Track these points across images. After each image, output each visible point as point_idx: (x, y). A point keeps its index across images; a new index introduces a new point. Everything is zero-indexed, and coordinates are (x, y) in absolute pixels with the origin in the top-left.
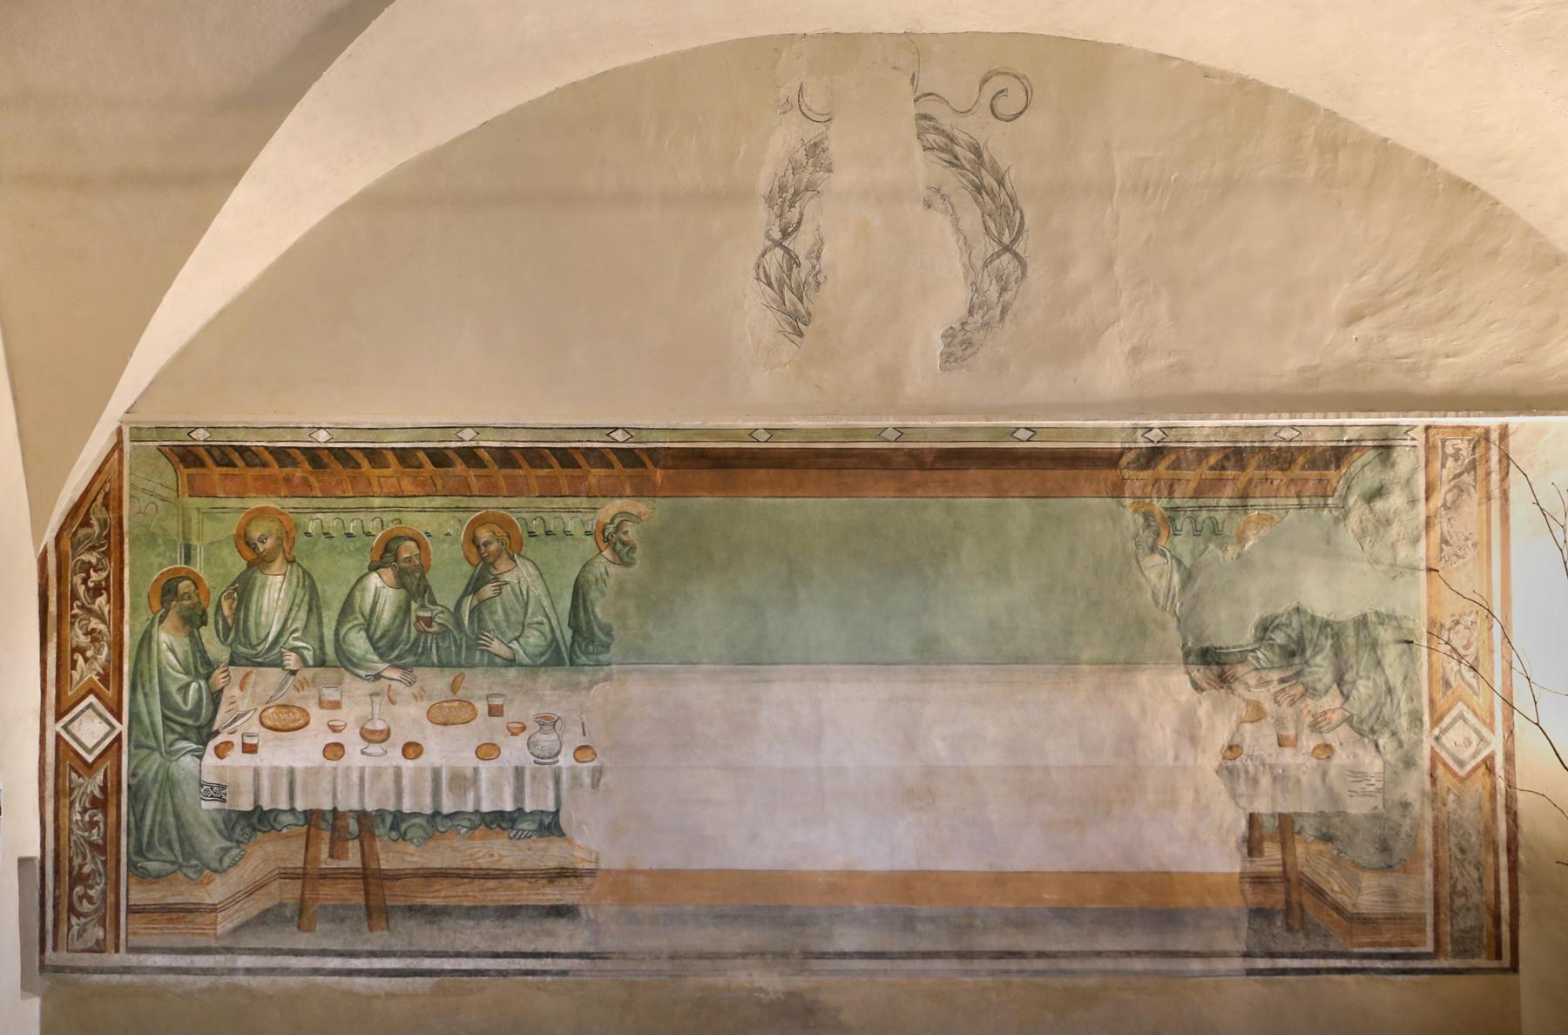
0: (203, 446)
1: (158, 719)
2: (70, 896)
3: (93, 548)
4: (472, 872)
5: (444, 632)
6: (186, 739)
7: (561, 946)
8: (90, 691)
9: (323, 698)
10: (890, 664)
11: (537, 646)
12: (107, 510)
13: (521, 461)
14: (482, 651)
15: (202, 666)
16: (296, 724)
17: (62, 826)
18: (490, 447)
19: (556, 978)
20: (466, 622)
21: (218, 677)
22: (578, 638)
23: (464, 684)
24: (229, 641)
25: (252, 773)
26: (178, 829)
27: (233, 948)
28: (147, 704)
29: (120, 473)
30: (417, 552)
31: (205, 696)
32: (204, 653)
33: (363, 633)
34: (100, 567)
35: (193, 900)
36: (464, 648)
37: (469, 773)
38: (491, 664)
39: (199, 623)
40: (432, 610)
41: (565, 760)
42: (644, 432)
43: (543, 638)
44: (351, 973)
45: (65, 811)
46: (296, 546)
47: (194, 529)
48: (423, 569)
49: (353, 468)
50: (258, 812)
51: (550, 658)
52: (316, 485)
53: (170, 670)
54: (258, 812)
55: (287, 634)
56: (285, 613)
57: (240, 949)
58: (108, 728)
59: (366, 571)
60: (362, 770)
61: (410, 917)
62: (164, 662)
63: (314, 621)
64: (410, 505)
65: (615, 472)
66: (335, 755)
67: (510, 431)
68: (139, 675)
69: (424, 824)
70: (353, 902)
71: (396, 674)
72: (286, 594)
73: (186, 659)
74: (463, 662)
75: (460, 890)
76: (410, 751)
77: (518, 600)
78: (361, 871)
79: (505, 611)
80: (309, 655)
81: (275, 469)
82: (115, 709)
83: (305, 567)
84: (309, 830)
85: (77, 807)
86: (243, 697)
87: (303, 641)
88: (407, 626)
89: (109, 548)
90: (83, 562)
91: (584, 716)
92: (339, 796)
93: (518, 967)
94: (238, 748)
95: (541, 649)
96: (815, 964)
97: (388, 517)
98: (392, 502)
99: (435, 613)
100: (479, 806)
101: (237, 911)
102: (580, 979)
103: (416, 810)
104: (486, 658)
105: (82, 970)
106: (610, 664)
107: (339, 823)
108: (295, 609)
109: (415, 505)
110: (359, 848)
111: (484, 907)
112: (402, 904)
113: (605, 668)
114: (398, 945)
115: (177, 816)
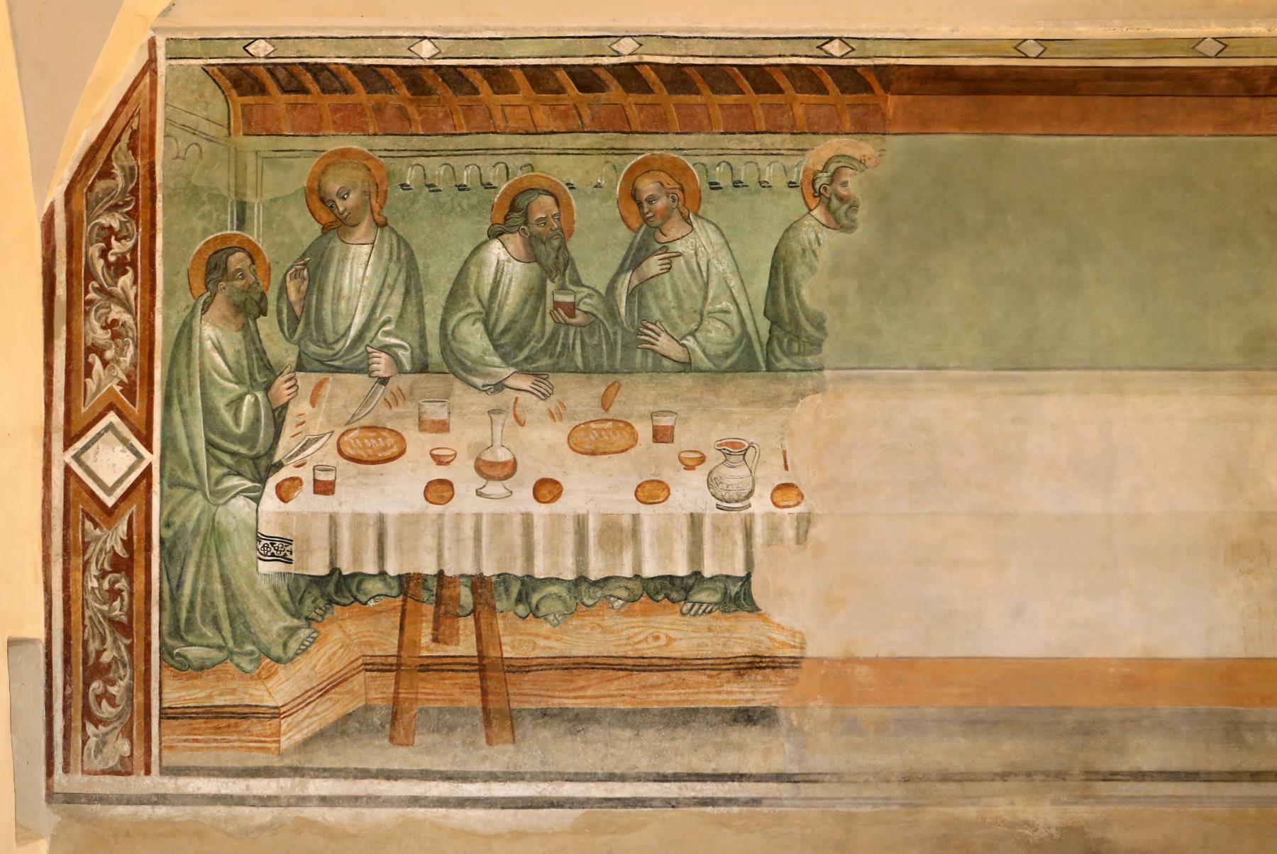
0: (264, 64)
1: (201, 445)
2: (85, 696)
3: (115, 207)
4: (630, 662)
5: (592, 323)
6: (239, 474)
7: (752, 765)
8: (111, 407)
9: (425, 417)
10: (1207, 370)
12: (135, 154)
13: (700, 84)
14: (645, 351)
15: (259, 372)
16: (388, 454)
17: (73, 597)
19: (745, 809)
20: (623, 310)
21: (282, 388)
22: (777, 332)
24: (296, 337)
26: (227, 602)
27: (303, 769)
28: (186, 425)
29: (153, 103)
30: (555, 210)
31: (263, 413)
32: (262, 353)
33: (479, 326)
34: (124, 233)
35: (247, 702)
36: (619, 346)
37: (626, 522)
38: (658, 369)
39: (255, 311)
40: (575, 293)
41: (761, 505)
42: (869, 44)
43: (729, 333)
44: (462, 803)
45: (77, 575)
46: (388, 203)
47: (251, 179)
48: (564, 235)
50: (335, 578)
51: (739, 358)
52: (417, 117)
53: (217, 377)
54: (335, 578)
55: (375, 328)
56: (372, 298)
57: (312, 769)
58: (134, 458)
59: (485, 237)
60: (478, 517)
61: (544, 725)
62: (208, 365)
63: (412, 308)
64: (546, 145)
67: (685, 42)
68: (175, 384)
69: (564, 594)
70: (465, 705)
71: (525, 383)
72: (375, 271)
73: (238, 362)
74: (618, 366)
75: (613, 687)
76: (544, 491)
77: (694, 278)
78: (476, 661)
80: (404, 356)
81: (361, 95)
82: (144, 432)
83: (400, 233)
84: (405, 601)
85: (94, 570)
86: (315, 416)
87: (397, 337)
88: (540, 314)
89: (136, 207)
90: (103, 228)
91: (786, 443)
93: (693, 794)
94: (308, 486)
95: (725, 348)
96: (1102, 788)
97: (515, 162)
98: (519, 141)
99: (579, 296)
100: (640, 570)
101: (307, 717)
102: (777, 810)
104: (650, 360)
105: (102, 800)
107: (446, 592)
108: (387, 292)
109: (552, 146)
110: (474, 629)
111: (644, 711)
112: (534, 707)
113: (815, 374)
114: (528, 763)
115: (226, 582)
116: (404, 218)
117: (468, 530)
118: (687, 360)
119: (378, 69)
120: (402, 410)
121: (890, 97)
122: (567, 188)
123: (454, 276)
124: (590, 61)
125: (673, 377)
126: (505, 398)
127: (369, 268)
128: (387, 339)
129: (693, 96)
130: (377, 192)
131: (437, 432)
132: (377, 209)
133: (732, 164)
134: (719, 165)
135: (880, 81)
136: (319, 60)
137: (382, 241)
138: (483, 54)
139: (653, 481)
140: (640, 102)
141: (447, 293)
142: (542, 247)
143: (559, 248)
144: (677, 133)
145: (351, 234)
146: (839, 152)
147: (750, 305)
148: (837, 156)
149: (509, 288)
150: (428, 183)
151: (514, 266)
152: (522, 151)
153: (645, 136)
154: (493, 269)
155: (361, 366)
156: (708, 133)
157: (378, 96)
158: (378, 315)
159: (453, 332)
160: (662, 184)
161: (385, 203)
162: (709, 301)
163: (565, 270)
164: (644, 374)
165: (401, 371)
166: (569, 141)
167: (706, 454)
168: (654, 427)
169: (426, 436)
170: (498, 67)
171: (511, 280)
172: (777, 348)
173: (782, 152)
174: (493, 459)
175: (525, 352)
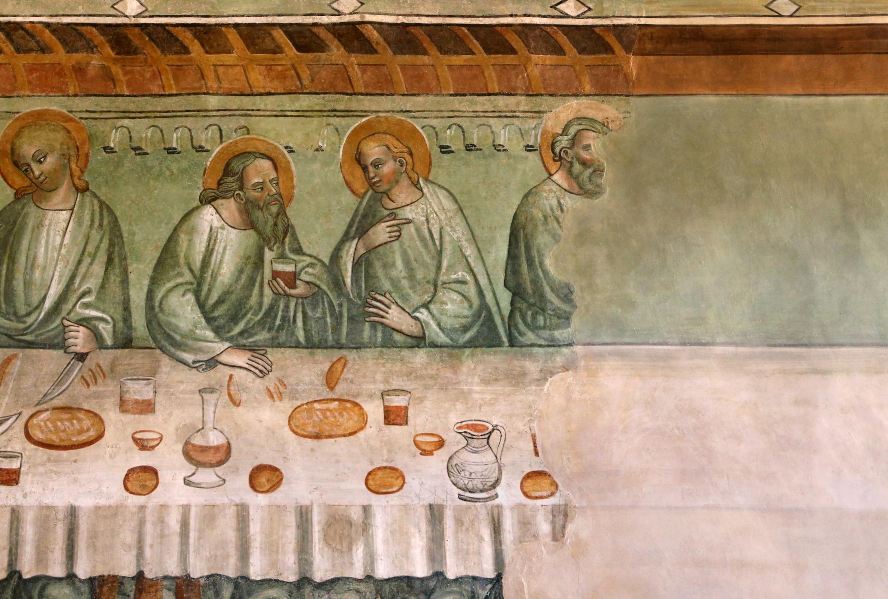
5: (315, 295)
9: (127, 397)
11: (456, 317)
13: (427, 43)
14: (374, 325)
16: (83, 438)
18: (381, 24)
20: (348, 281)
23: (347, 375)
25: (7, 516)
30: (273, 175)
33: (190, 297)
36: (345, 319)
37: (356, 515)
38: (389, 343)
40: (296, 263)
43: (466, 305)
46: (89, 167)
48: (283, 201)
51: (478, 332)
55: (73, 299)
56: (71, 267)
59: (197, 203)
60: (186, 510)
63: (115, 278)
64: (262, 107)
65: (566, 59)
66: (144, 487)
71: (240, 358)
72: (74, 238)
74: (343, 341)
76: (263, 479)
77: (426, 246)
79: (407, 263)
80: (106, 331)
81: (60, 55)
87: (98, 309)
88: (257, 284)
92: (148, 552)
95: (463, 321)
97: (229, 124)
98: (235, 102)
99: (300, 266)
100: (373, 570)
103: (271, 576)
104: (379, 334)
106: (570, 345)
108: (87, 260)
109: (269, 107)
116: (107, 182)
117: (173, 522)
118: (421, 335)
119: (78, 28)
120: (101, 389)
121: (632, 57)
122: (285, 151)
123: (162, 244)
124: (309, 20)
125: (405, 352)
126: (219, 375)
127: (68, 235)
128: (87, 311)
129: (420, 56)
130: (78, 155)
131: (141, 412)
132: (77, 173)
133: (464, 127)
134: (449, 128)
135: (620, 41)
136: (12, 19)
137: (82, 206)
138: (193, 13)
139: (385, 468)
140: (363, 62)
141: (155, 262)
142: (259, 214)
143: (278, 214)
144: (403, 95)
145: (47, 199)
146: (580, 115)
147: (488, 275)
148: (578, 119)
149: (222, 257)
150: (135, 145)
151: (228, 233)
152: (237, 113)
153: (369, 97)
154: (205, 237)
155: (56, 341)
156: (437, 95)
157: (79, 57)
158: (76, 285)
159: (161, 303)
160: (388, 148)
161: (86, 167)
162: (443, 270)
163: (284, 238)
164: (372, 350)
165: (101, 345)
166: (287, 103)
167: (445, 437)
168: (385, 407)
169: (129, 417)
170: (210, 25)
171: (225, 248)
172: (520, 321)
173: (517, 114)
174: (204, 444)
175: (241, 326)
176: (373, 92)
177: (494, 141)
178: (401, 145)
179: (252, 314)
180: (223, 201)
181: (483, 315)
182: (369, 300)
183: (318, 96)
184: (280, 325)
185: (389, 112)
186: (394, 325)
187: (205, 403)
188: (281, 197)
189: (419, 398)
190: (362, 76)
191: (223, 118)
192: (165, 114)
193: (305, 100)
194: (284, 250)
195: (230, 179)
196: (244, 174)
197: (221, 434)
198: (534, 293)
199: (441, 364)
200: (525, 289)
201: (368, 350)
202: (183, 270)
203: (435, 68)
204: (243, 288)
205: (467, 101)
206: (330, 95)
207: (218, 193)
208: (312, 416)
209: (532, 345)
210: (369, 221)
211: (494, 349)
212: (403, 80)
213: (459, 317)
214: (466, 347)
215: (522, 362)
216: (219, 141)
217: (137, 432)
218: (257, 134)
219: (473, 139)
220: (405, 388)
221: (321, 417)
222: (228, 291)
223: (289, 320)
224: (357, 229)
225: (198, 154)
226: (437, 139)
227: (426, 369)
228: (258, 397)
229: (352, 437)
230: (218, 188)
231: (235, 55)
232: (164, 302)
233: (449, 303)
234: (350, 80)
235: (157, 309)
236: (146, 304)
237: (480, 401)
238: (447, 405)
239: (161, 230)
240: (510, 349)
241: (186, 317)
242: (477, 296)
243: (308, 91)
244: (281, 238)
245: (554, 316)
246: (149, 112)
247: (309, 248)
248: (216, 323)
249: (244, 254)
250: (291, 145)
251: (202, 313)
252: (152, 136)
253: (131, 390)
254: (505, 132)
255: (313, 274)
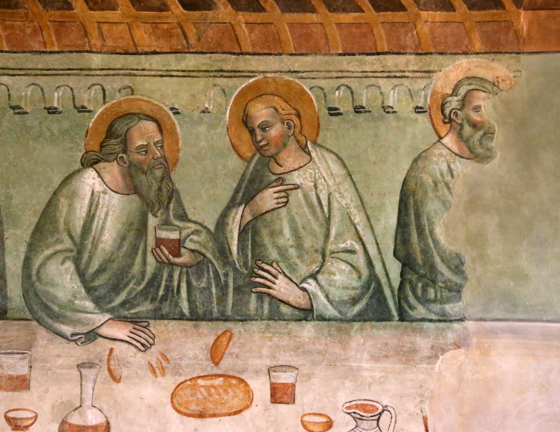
14: (261, 296)
20: (234, 249)
23: (233, 349)
30: (158, 138)
33: (69, 265)
36: (231, 290)
40: (180, 229)
43: (355, 276)
49: (58, 9)
51: (367, 304)
59: (78, 166)
64: (147, 66)
74: (229, 312)
77: (314, 213)
79: (295, 231)
88: (140, 252)
95: (352, 293)
98: (119, 61)
99: (185, 233)
104: (266, 306)
109: (155, 67)
118: (309, 307)
122: (171, 113)
123: (40, 208)
125: (293, 326)
126: (98, 349)
129: (309, 15)
131: (15, 389)
133: (353, 88)
134: (338, 88)
140: (251, 20)
141: (33, 227)
142: (143, 178)
143: (163, 179)
144: (291, 55)
147: (377, 244)
149: (104, 223)
150: (13, 104)
152: (121, 72)
153: (256, 57)
154: (87, 201)
156: (325, 54)
159: (38, 272)
160: (276, 109)
162: (332, 239)
163: (169, 203)
167: (333, 418)
168: (272, 384)
171: (107, 214)
172: (410, 294)
173: (407, 74)
174: (81, 423)
176: (260, 52)
177: (383, 103)
178: (288, 106)
179: (135, 284)
180: (106, 164)
181: (373, 286)
182: (256, 270)
183: (205, 56)
184: (163, 295)
185: (276, 72)
186: (280, 297)
187: (84, 379)
188: (166, 161)
189: (307, 374)
190: (250, 35)
191: (106, 78)
192: (46, 72)
193: (191, 59)
194: (168, 215)
195: (113, 141)
196: (128, 138)
197: (100, 413)
198: (424, 264)
199: (329, 338)
200: (415, 259)
201: (254, 322)
202: (63, 237)
203: (324, 27)
204: (125, 255)
205: (356, 60)
206: (217, 55)
207: (100, 155)
208: (196, 394)
209: (423, 320)
210: (256, 187)
211: (384, 323)
212: (291, 39)
213: (347, 288)
214: (355, 321)
215: (413, 338)
216: (102, 102)
217: (10, 411)
218: (142, 95)
219: (362, 101)
220: (292, 364)
221: (205, 394)
222: (110, 259)
223: (173, 290)
224: (244, 195)
225: (80, 114)
226: (326, 101)
227: (314, 344)
228: (139, 372)
229: (237, 416)
230: (101, 151)
231: (119, 12)
232: (42, 271)
233: (337, 273)
234: (237, 39)
235: (34, 278)
236: (23, 272)
237: (369, 379)
238: (335, 383)
239: (40, 194)
240: (400, 323)
241: (64, 287)
242: (366, 267)
243: (194, 50)
244: (165, 204)
245: (445, 288)
246: (30, 69)
247: (194, 214)
248: (97, 293)
249: (127, 220)
250: (176, 107)
251: (82, 282)
252: (32, 95)
253: (5, 365)
254: (394, 93)
255: (198, 242)
